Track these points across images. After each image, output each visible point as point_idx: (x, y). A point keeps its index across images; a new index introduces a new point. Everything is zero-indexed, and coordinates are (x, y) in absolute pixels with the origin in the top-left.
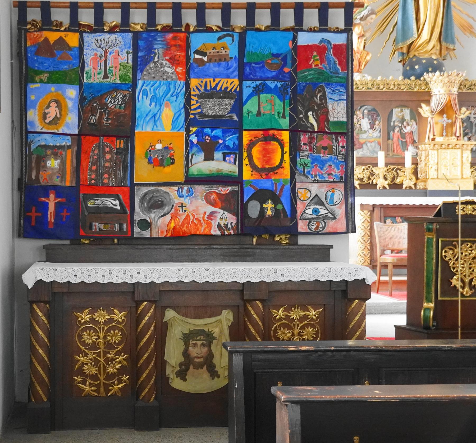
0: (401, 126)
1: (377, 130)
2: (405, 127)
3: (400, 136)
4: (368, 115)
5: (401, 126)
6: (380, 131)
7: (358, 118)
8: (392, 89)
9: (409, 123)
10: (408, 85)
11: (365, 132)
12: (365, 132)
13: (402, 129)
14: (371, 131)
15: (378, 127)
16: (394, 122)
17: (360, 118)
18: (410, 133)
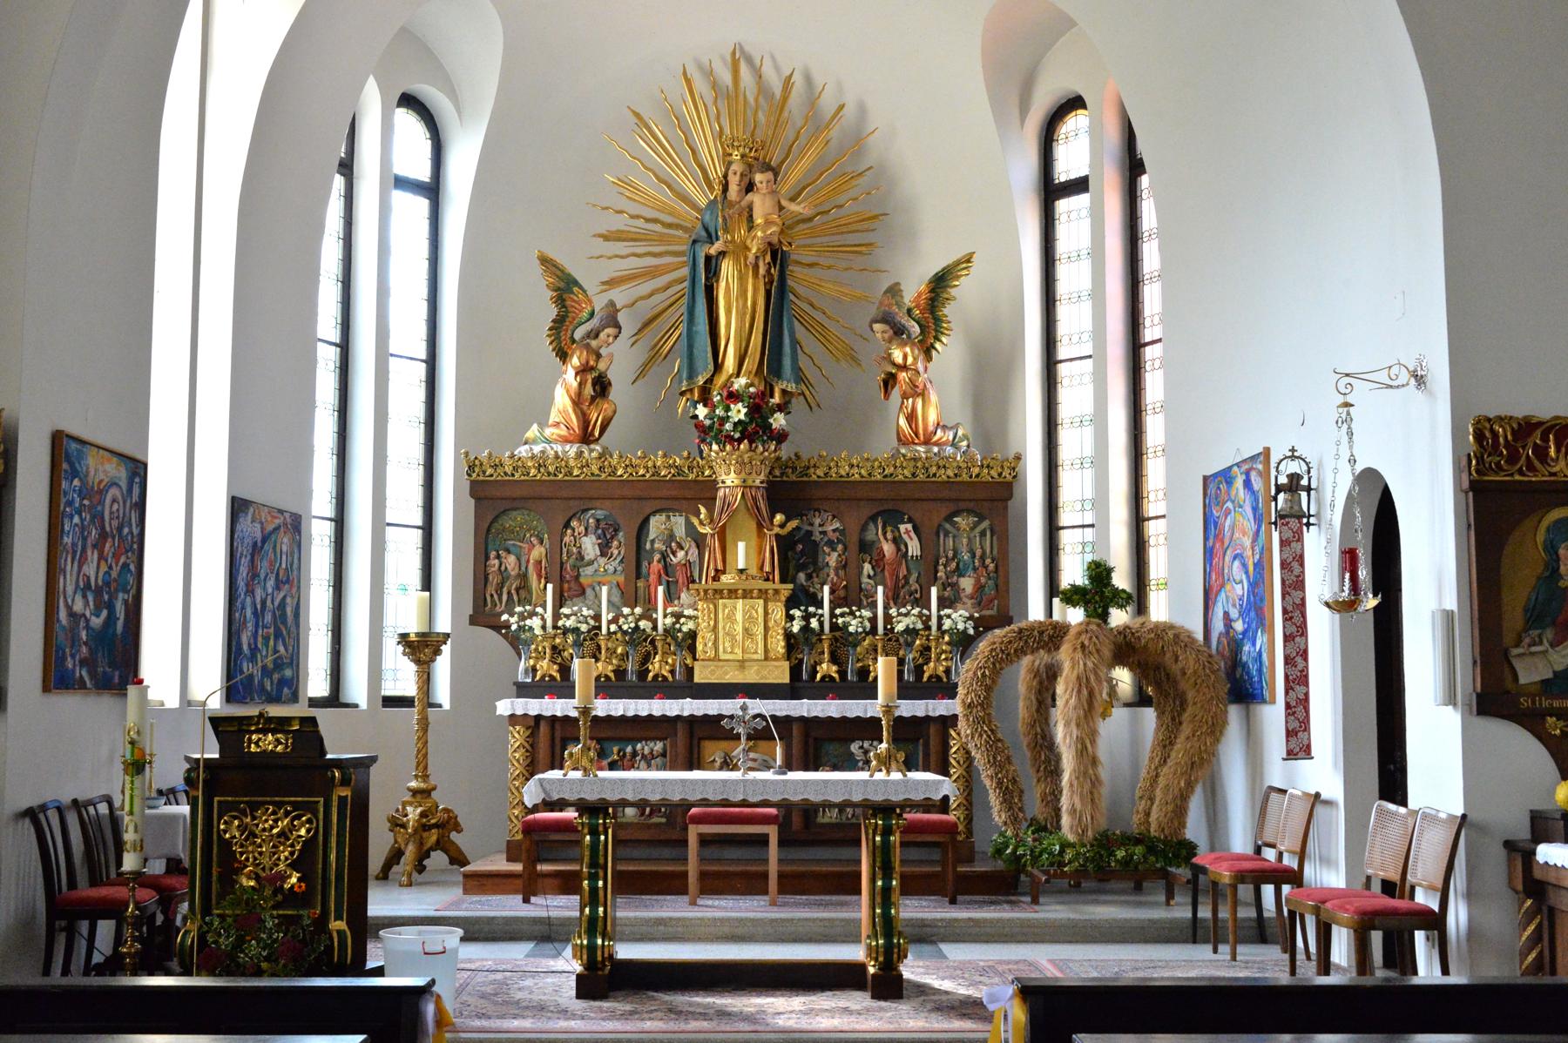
2: (674, 553)
4: (597, 527)
6: (622, 561)
7: (576, 534)
8: (644, 476)
9: (683, 545)
11: (591, 563)
12: (591, 563)
13: (668, 556)
14: (602, 561)
15: (616, 552)
16: (653, 542)
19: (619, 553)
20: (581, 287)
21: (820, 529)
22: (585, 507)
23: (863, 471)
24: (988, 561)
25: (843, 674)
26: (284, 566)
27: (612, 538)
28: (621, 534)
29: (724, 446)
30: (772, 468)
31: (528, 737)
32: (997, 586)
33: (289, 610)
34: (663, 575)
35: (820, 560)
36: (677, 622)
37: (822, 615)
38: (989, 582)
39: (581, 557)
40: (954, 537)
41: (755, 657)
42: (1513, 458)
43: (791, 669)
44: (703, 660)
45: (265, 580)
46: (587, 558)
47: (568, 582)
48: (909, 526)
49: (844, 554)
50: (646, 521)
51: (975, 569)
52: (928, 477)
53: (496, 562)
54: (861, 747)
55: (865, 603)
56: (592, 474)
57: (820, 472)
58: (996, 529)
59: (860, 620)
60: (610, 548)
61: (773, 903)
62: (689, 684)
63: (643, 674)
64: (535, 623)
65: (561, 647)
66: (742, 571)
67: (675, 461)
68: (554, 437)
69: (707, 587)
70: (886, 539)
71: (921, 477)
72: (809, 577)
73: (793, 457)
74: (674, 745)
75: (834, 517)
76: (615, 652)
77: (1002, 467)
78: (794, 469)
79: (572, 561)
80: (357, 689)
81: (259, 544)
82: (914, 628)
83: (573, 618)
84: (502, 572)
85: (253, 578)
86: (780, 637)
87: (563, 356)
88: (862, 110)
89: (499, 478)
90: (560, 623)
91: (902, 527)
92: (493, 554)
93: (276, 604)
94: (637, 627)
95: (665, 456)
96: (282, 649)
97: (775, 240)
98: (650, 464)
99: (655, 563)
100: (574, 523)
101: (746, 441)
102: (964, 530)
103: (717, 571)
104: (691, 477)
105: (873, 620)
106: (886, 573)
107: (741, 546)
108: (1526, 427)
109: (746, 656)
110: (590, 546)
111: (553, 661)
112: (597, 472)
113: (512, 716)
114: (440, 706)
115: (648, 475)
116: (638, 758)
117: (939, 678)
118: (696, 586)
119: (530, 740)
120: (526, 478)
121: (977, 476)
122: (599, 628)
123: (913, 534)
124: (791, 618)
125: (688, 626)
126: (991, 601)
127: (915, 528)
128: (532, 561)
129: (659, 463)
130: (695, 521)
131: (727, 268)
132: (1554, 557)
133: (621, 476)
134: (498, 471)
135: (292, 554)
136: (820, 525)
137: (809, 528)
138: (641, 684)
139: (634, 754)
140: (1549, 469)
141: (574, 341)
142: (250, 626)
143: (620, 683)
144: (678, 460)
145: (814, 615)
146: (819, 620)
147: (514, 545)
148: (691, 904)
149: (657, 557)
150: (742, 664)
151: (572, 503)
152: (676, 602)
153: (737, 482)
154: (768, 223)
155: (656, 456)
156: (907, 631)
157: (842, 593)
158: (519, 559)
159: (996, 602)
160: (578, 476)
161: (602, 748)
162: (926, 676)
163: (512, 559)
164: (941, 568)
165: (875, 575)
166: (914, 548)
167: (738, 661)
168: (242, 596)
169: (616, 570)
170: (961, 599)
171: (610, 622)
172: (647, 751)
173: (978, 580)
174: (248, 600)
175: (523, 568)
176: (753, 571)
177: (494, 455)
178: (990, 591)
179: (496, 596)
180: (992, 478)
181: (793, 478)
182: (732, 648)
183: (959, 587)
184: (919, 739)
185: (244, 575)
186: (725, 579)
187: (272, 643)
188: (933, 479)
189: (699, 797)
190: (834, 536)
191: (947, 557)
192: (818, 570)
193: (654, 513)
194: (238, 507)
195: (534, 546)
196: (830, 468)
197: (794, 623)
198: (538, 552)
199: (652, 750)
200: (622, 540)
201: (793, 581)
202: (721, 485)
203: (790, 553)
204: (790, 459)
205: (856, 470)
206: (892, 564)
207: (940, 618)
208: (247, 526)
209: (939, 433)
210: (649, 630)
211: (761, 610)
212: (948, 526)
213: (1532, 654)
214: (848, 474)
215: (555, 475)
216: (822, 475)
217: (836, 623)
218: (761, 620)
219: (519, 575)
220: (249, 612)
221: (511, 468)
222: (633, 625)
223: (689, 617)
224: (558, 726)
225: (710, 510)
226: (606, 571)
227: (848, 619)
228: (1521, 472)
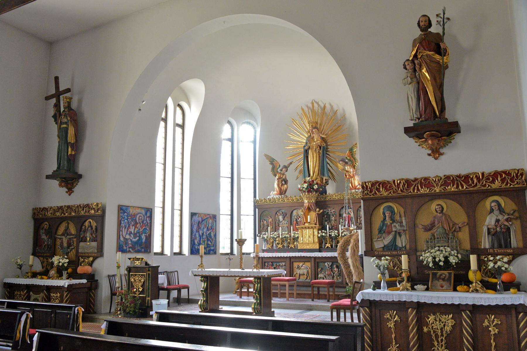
4: (282, 214)
14: (283, 221)
16: (294, 216)
20: (276, 160)
26: (210, 226)
33: (212, 235)
35: (331, 218)
39: (279, 221)
42: (371, 192)
45: (203, 229)
50: (292, 212)
53: (262, 222)
54: (328, 264)
61: (288, 300)
66: (309, 222)
80: (167, 252)
81: (201, 222)
84: (263, 225)
85: (199, 229)
87: (275, 176)
88: (344, 110)
93: (207, 234)
96: (210, 243)
97: (319, 144)
100: (278, 213)
105: (279, 234)
108: (373, 184)
110: (281, 218)
114: (235, 255)
131: (310, 151)
132: (384, 216)
135: (213, 223)
137: (328, 211)
139: (279, 265)
140: (380, 193)
141: (278, 172)
142: (198, 239)
143: (332, 249)
148: (287, 300)
149: (295, 220)
154: (317, 140)
164: (358, 219)
168: (195, 232)
169: (286, 223)
174: (197, 233)
181: (323, 200)
185: (196, 228)
187: (206, 242)
189: (237, 275)
190: (333, 213)
194: (192, 215)
198: (270, 220)
208: (196, 218)
213: (378, 240)
218: (312, 234)
220: (197, 236)
224: (263, 259)
228: (373, 195)
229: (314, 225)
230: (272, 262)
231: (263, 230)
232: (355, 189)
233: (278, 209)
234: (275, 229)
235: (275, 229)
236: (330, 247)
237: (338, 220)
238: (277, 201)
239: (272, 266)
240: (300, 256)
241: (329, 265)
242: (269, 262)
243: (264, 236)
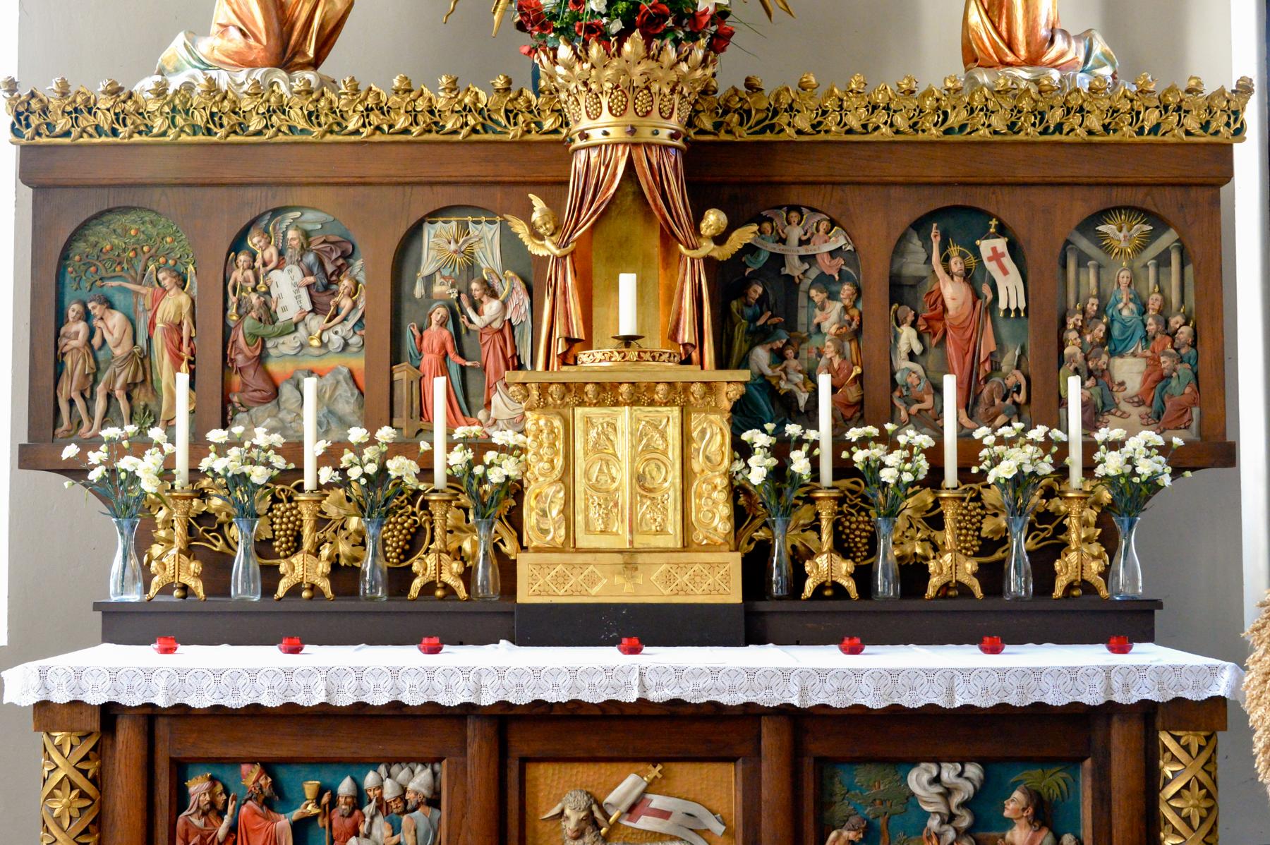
0: (458, 299)
1: (345, 319)
3: (449, 347)
4: (304, 249)
5: (458, 299)
8: (406, 131)
9: (497, 286)
10: (481, 112)
14: (316, 323)
15: (346, 303)
16: (429, 280)
17: (265, 264)
18: (501, 331)
19: (355, 305)
21: (803, 251)
22: (276, 205)
23: (899, 120)
24: (1176, 321)
25: (864, 576)
27: (339, 271)
28: (358, 264)
29: (586, 45)
30: (696, 112)
31: (86, 758)
32: (1196, 376)
34: (452, 355)
35: (802, 317)
36: (478, 460)
37: (815, 444)
38: (1179, 366)
39: (268, 315)
40: (1099, 267)
41: (660, 542)
43: (747, 562)
44: (538, 550)
46: (282, 317)
47: (241, 370)
48: (1001, 244)
49: (854, 306)
50: (415, 232)
51: (1147, 338)
52: (1045, 132)
53: (81, 327)
55: (903, 414)
56: (290, 128)
57: (803, 122)
58: (1196, 249)
59: (906, 454)
60: (334, 294)
62: (506, 606)
63: (399, 578)
64: (146, 468)
65: (222, 517)
66: (628, 341)
67: (477, 99)
68: (217, 55)
69: (547, 377)
70: (948, 272)
71: (1030, 132)
72: (778, 357)
73: (742, 88)
74: (459, 774)
75: (833, 223)
76: (343, 528)
77: (1210, 110)
78: (745, 114)
79: (249, 322)
82: (1033, 474)
83: (234, 452)
86: (721, 496)
89: (86, 139)
90: (204, 465)
91: (986, 246)
92: (73, 310)
94: (383, 470)
95: (453, 87)
98: (421, 105)
99: (434, 327)
100: (254, 241)
101: (636, 34)
102: (1121, 252)
103: (570, 341)
104: (514, 132)
106: (951, 349)
107: (627, 282)
109: (640, 542)
111: (189, 551)
112: (302, 124)
113: (43, 706)
115: (416, 130)
116: (369, 809)
117: (1087, 587)
118: (520, 376)
119: (92, 768)
120: (144, 138)
121: (1155, 129)
122: (299, 472)
123: (1007, 261)
124: (743, 450)
125: (501, 470)
126: (1185, 410)
127: (1013, 248)
128: (159, 325)
129: (440, 104)
130: (521, 229)
133: (357, 132)
134: (82, 122)
136: (801, 243)
137: (778, 248)
138: (396, 605)
139: (359, 799)
144: (483, 96)
145: (799, 442)
146: (809, 454)
147: (122, 290)
149: (439, 313)
150: (630, 557)
151: (250, 193)
152: (481, 415)
153: (616, 134)
155: (434, 89)
156: (1020, 481)
157: (853, 394)
158: (132, 322)
159: (1196, 411)
160: (259, 133)
161: (276, 786)
162: (1060, 584)
163: (115, 320)
164: (1072, 335)
165: (924, 352)
166: (1010, 290)
167: (621, 552)
169: (346, 345)
170: (1117, 406)
171: (322, 461)
172: (389, 791)
173: (1154, 362)
175: (142, 341)
176: (655, 342)
177: (73, 90)
178: (1180, 388)
179: (80, 404)
180: (1188, 133)
181: (743, 135)
182: (606, 524)
183: (1111, 379)
184: (1083, 759)
186: (594, 361)
188: (1057, 137)
190: (832, 267)
191: (1084, 311)
192: (796, 341)
193: (434, 215)
195: (165, 291)
196: (825, 113)
197: (751, 461)
198: (173, 304)
199: (404, 790)
200: (361, 277)
201: (743, 363)
202: (579, 143)
203: (735, 305)
204: (736, 91)
205: (881, 117)
206: (961, 328)
207: (1090, 448)
209: (1060, 43)
210: (411, 482)
211: (673, 432)
212: (1084, 244)
214: (865, 126)
215: (209, 132)
216: (808, 129)
217: (850, 461)
218: (674, 454)
219: (131, 355)
221: (110, 116)
222: (371, 469)
223: (503, 449)
224: (162, 728)
225: (554, 205)
226: (324, 345)
227: (877, 451)
229: (674, 372)
230: (268, 767)
231: (89, 401)
232: (1033, 60)
233: (259, 200)
234: (226, 401)
235: (226, 401)
236: (849, 584)
237: (873, 329)
238: (255, 124)
239: (268, 803)
240: (632, 697)
241: (947, 793)
242: (236, 762)
243: (127, 463)
